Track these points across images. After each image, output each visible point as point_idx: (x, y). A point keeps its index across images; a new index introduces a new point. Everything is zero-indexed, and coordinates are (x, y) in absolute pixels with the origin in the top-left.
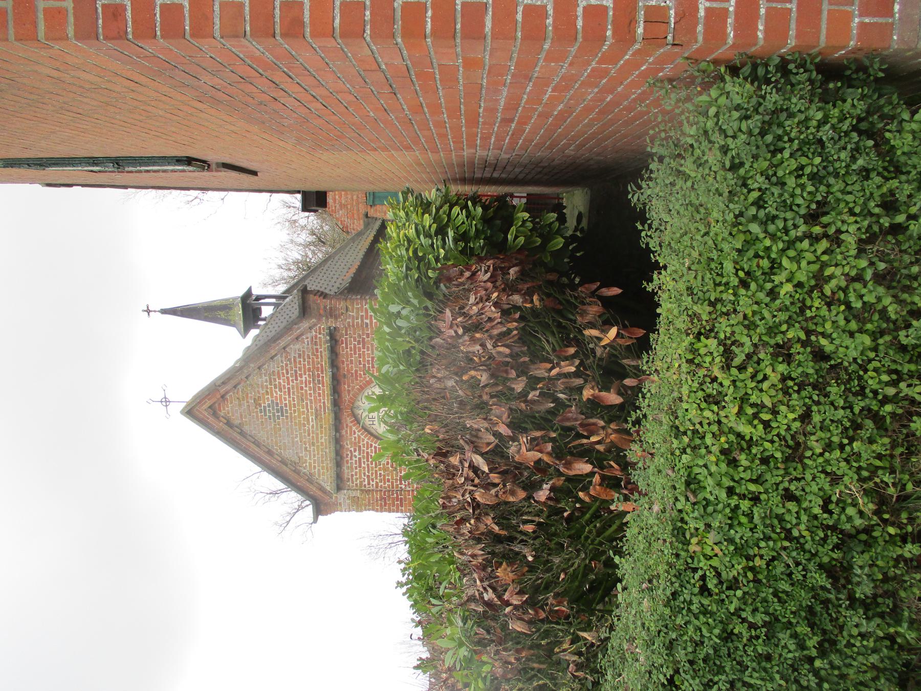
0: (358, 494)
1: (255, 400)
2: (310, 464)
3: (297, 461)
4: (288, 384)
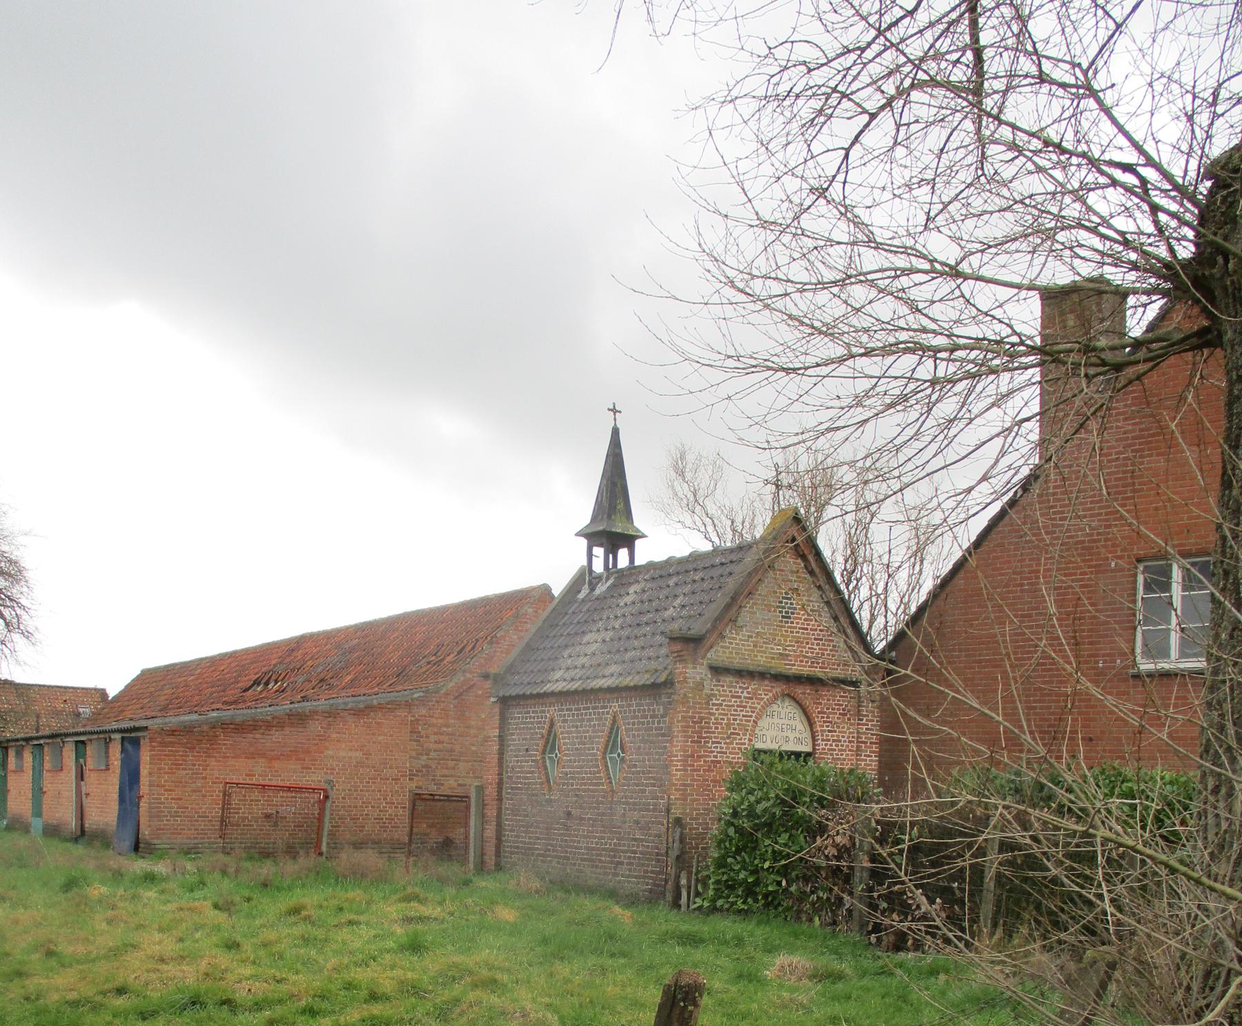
0: (707, 691)
1: (797, 589)
2: (734, 639)
3: (738, 624)
4: (811, 630)
